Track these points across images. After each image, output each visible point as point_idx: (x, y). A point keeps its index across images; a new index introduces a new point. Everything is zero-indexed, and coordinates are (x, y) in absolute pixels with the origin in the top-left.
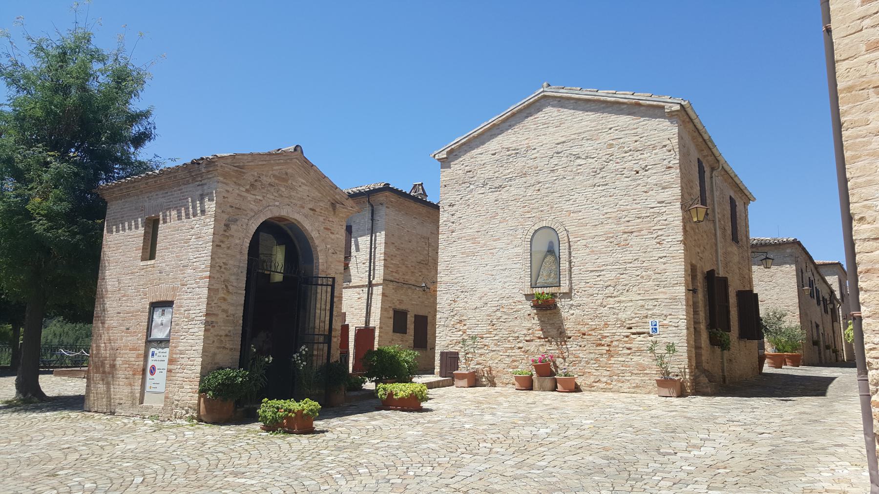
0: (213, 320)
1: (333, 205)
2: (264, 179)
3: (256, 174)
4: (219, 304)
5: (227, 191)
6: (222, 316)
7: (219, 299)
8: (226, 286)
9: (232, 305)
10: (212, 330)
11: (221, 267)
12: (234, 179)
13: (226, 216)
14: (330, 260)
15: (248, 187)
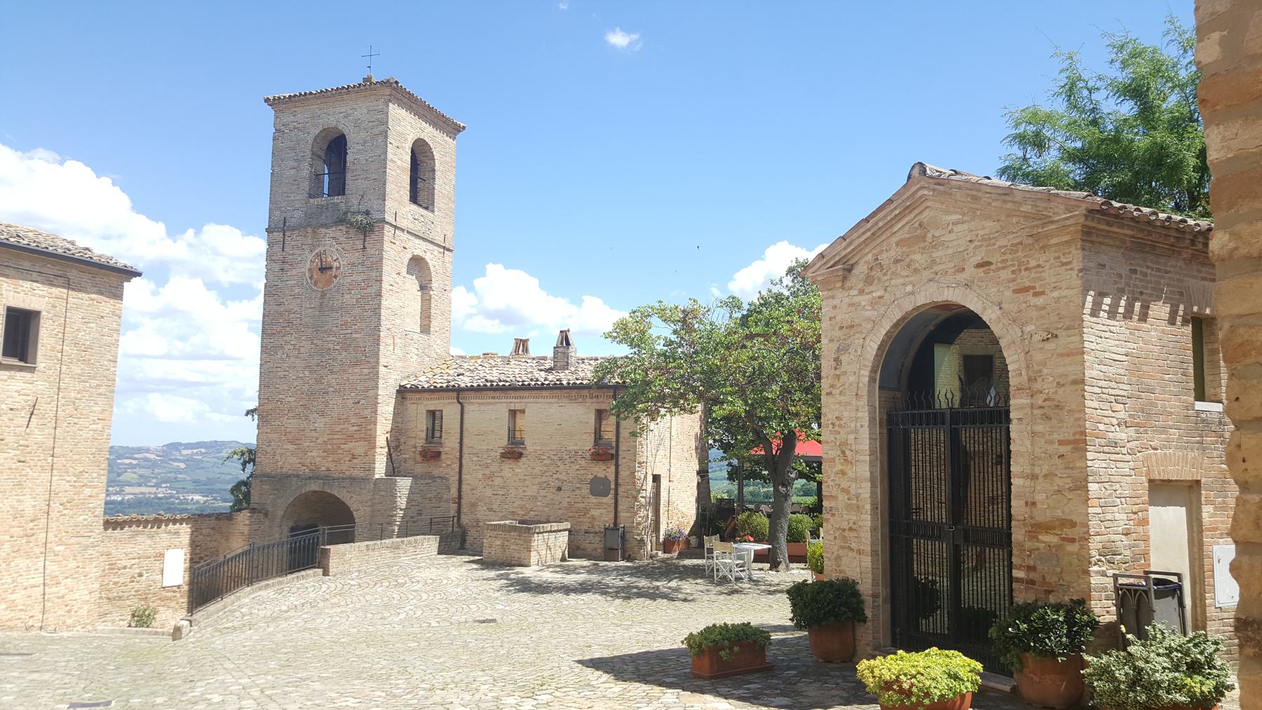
2: (885, 258)
5: (835, 307)
8: (843, 452)
9: (855, 480)
13: (834, 346)
14: (1038, 357)
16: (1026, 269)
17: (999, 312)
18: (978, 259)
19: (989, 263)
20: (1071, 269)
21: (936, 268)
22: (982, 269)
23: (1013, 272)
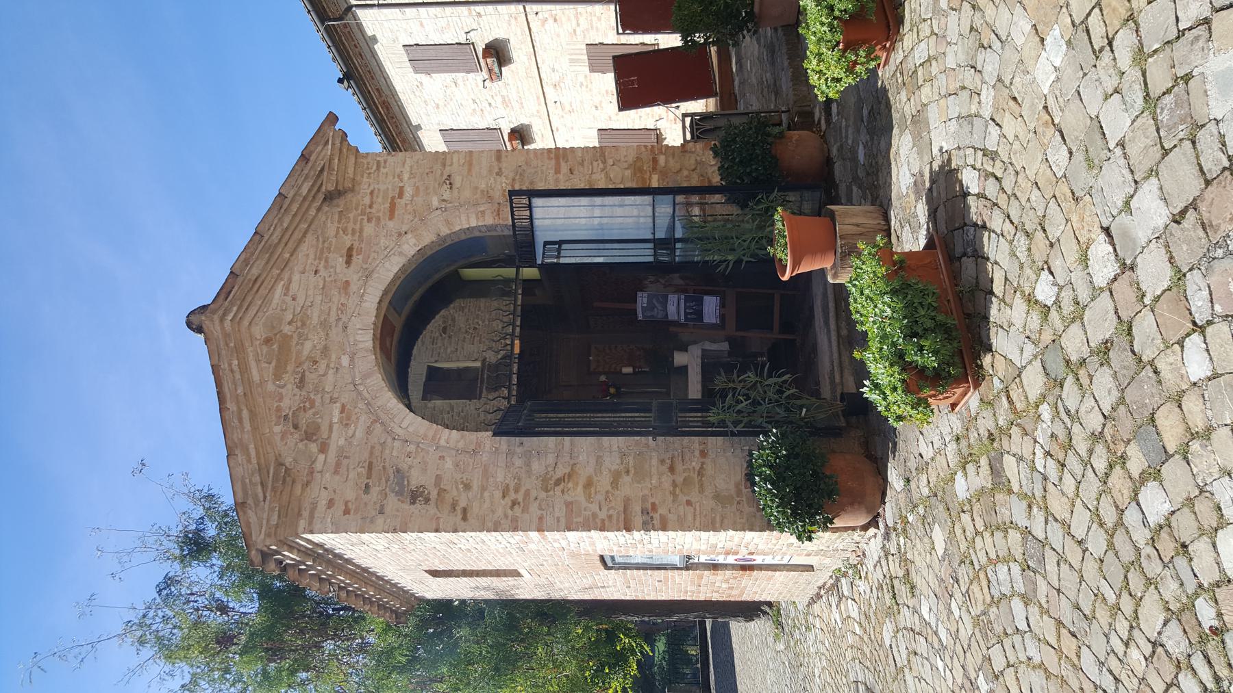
0: (638, 509)
1: (330, 197)
2: (288, 403)
3: (277, 429)
4: (601, 497)
5: (331, 503)
6: (628, 487)
7: (589, 498)
8: (558, 482)
9: (599, 460)
10: (662, 511)
11: (514, 503)
12: (298, 490)
13: (392, 502)
14: (467, 194)
15: (314, 447)
16: (371, 207)
17: (409, 236)
18: (341, 261)
19: (350, 249)
20: (385, 162)
21: (332, 319)
22: (354, 258)
23: (369, 220)
